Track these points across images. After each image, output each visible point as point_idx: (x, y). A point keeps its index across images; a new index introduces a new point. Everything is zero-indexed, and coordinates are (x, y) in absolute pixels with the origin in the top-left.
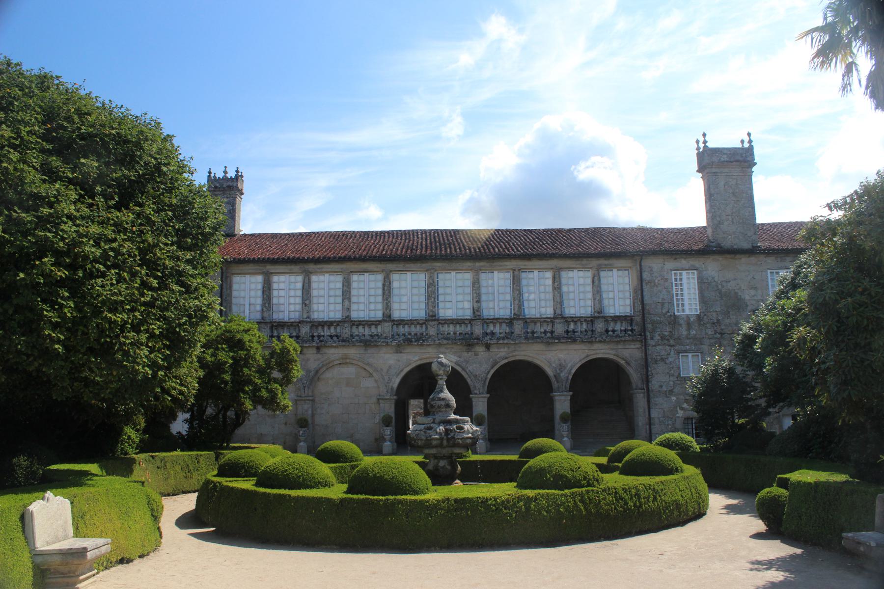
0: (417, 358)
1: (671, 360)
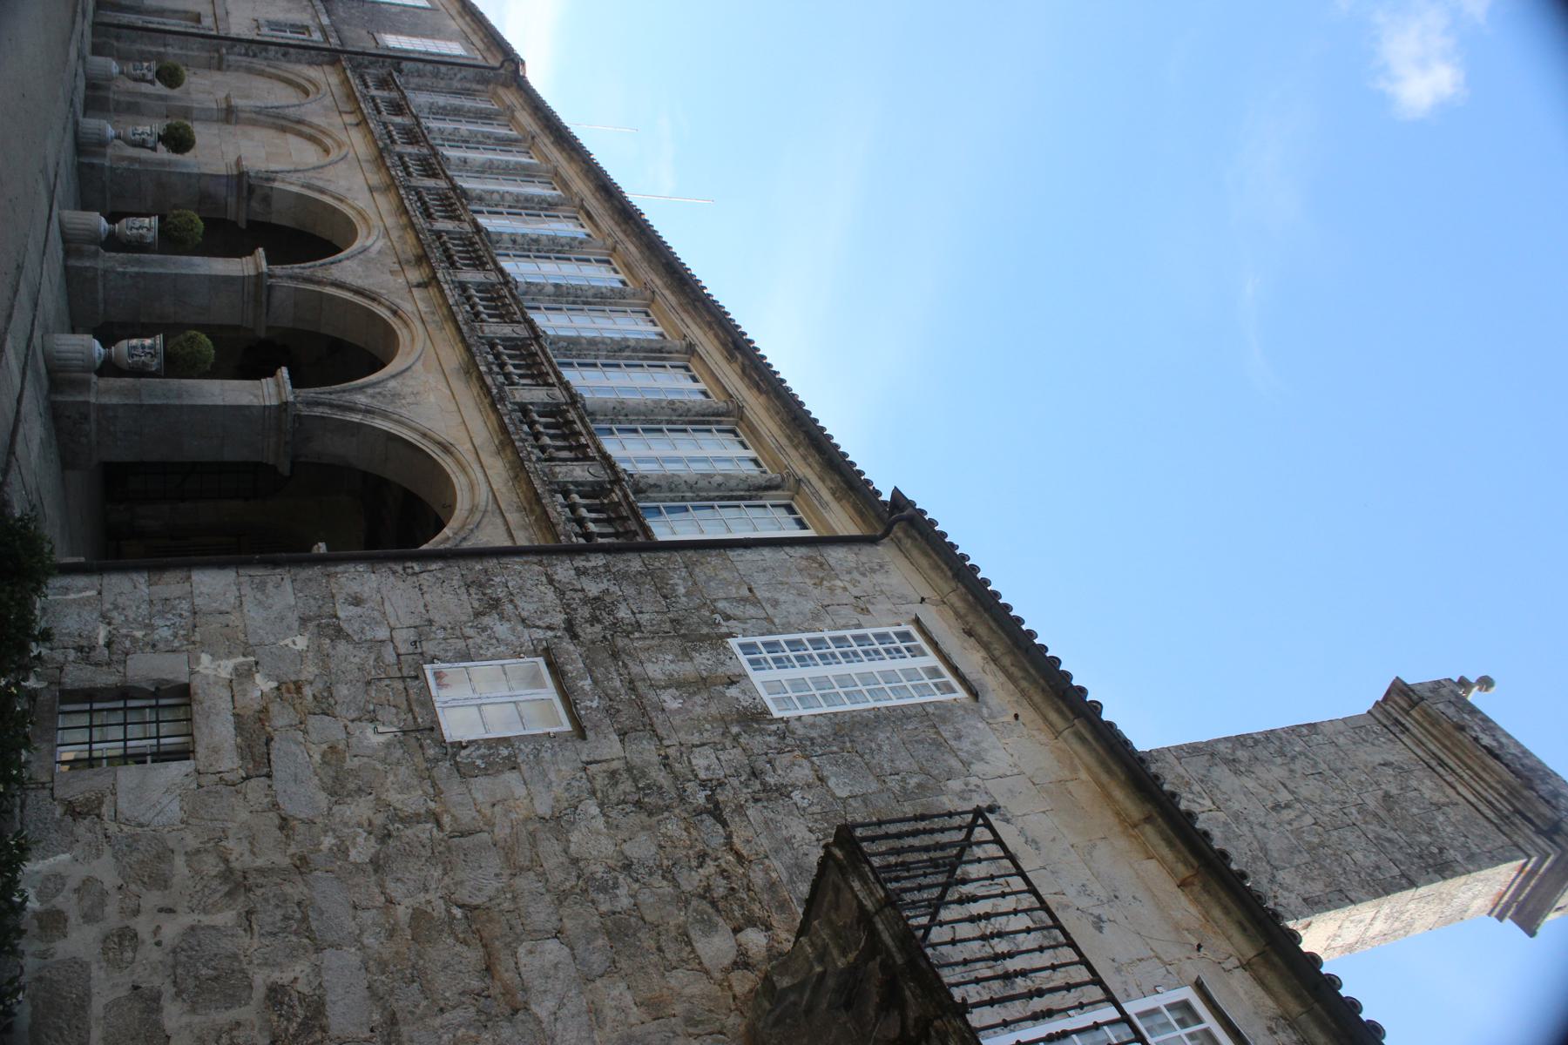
0: (360, 204)
1: (502, 629)
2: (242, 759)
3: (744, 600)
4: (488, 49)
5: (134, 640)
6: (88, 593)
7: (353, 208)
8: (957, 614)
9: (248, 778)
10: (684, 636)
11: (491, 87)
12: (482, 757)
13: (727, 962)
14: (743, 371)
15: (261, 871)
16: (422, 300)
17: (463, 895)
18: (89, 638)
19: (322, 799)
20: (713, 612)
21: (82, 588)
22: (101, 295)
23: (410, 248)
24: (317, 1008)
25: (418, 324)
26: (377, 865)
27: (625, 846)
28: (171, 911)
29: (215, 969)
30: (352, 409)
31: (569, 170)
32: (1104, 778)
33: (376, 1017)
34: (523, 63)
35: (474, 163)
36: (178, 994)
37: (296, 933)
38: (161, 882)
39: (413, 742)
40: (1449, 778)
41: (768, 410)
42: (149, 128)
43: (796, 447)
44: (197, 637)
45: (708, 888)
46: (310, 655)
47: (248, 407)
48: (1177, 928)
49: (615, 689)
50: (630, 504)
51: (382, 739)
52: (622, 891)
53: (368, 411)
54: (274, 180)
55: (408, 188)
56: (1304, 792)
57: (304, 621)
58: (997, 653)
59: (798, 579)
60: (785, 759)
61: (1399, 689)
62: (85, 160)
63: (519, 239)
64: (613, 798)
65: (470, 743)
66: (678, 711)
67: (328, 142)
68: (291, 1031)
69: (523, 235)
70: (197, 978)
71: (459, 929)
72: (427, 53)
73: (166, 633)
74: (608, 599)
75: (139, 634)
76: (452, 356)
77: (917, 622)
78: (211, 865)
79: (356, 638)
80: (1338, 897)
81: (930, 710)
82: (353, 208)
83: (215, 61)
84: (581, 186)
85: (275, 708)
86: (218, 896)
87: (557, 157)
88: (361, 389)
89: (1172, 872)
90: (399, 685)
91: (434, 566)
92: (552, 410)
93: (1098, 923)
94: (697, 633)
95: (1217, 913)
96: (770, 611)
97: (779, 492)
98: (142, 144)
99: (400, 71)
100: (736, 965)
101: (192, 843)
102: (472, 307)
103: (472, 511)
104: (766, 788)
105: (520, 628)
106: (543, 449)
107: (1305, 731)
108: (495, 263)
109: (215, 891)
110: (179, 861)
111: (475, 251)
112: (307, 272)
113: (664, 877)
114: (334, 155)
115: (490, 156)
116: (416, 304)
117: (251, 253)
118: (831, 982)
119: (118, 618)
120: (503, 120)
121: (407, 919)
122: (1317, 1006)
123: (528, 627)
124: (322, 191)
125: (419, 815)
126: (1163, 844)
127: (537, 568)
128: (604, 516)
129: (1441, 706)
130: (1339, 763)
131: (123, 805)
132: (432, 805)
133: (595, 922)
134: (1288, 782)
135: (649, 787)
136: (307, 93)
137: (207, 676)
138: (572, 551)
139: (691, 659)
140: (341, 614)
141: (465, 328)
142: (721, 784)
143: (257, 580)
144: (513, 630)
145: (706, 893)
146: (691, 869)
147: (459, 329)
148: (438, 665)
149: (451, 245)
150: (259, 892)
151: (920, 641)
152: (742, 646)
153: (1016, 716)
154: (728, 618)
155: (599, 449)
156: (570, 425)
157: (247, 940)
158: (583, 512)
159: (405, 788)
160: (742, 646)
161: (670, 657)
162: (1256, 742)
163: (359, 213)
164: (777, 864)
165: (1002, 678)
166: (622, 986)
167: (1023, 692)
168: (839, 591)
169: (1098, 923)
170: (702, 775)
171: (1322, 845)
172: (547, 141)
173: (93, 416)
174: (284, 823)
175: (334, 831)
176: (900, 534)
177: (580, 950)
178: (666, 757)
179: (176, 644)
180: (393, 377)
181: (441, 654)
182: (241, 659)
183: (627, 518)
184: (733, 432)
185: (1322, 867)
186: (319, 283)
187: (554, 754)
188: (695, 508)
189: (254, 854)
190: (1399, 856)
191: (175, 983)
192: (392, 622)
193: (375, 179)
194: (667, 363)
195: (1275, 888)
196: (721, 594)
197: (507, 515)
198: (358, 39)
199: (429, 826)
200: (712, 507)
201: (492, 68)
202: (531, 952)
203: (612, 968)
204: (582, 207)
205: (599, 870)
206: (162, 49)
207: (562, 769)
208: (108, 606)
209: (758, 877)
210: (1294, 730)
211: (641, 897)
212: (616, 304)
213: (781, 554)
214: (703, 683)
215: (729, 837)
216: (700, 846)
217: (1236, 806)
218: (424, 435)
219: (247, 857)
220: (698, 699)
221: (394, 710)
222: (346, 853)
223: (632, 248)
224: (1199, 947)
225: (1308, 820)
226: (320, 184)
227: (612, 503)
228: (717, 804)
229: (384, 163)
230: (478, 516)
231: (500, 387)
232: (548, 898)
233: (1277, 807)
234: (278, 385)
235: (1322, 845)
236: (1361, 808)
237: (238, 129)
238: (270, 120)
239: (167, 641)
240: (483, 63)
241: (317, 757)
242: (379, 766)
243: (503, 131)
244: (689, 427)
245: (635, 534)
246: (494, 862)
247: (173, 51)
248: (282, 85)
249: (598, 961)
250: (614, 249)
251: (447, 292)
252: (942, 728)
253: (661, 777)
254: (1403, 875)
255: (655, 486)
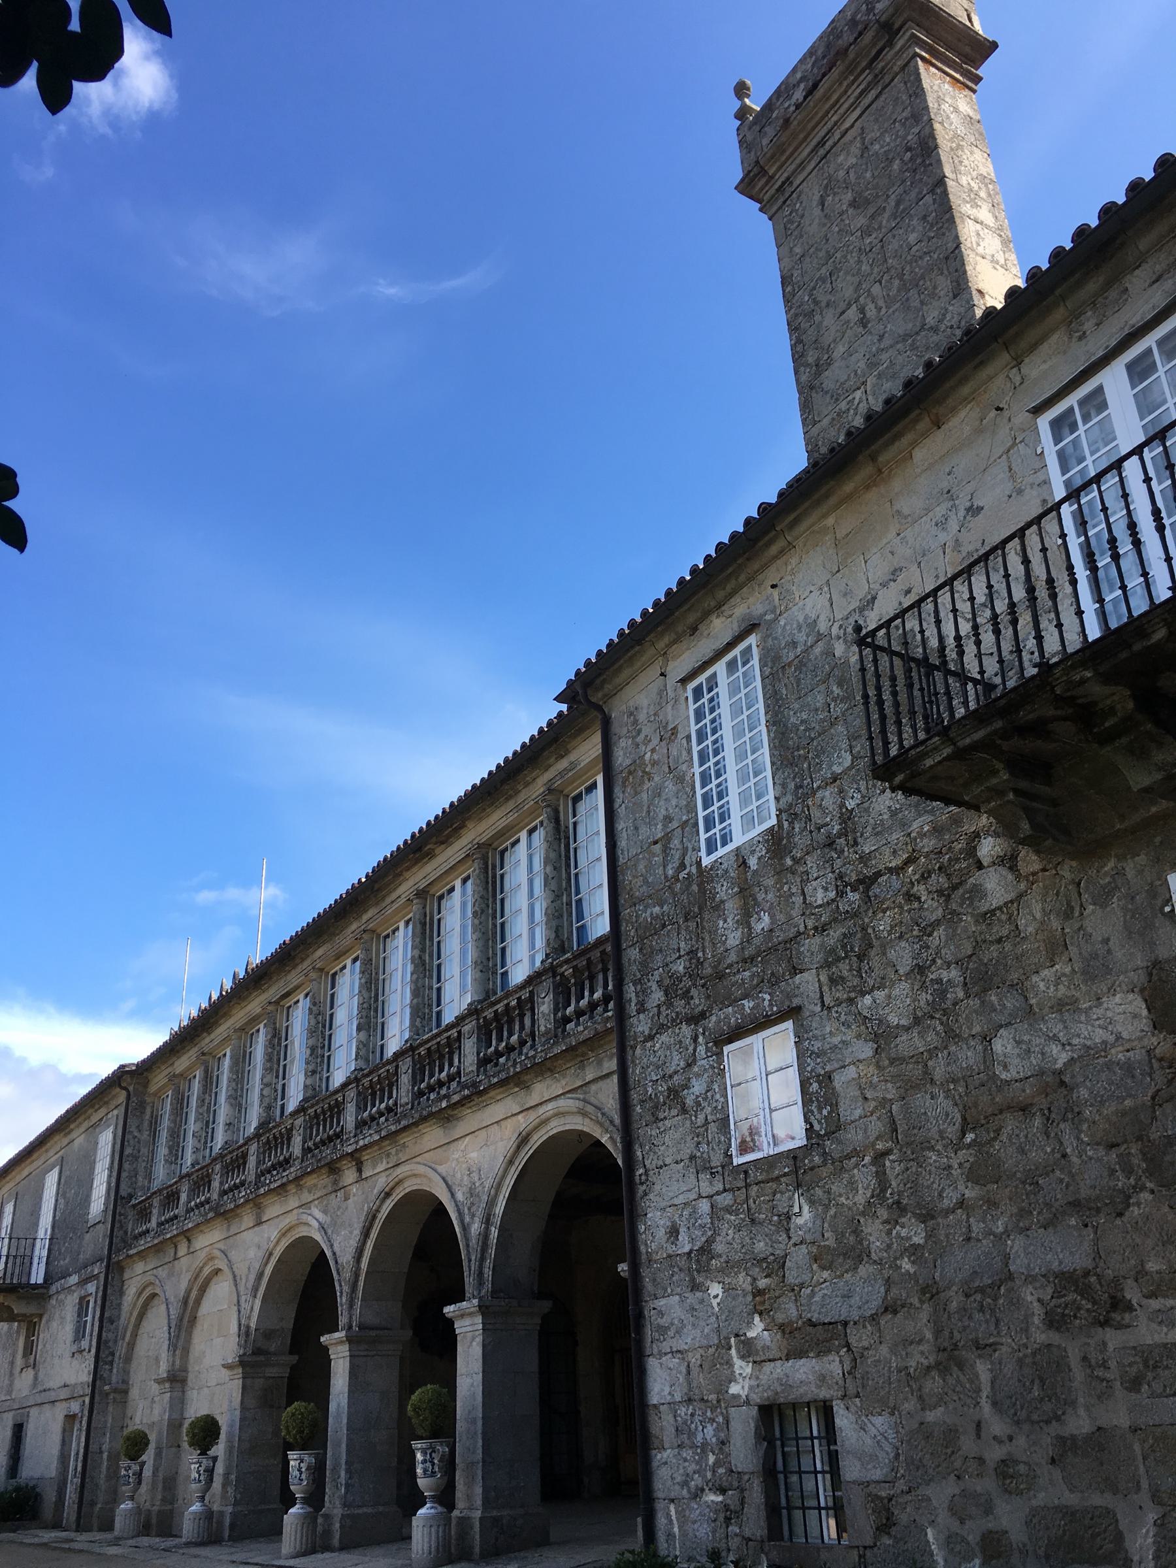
0: (274, 1235)
1: (698, 1087)
2: (829, 1351)
3: (666, 850)
4: (106, 1103)
5: (717, 1464)
6: (673, 1513)
7: (277, 1243)
8: (675, 642)
9: (848, 1345)
10: (700, 909)
11: (149, 1100)
12: (820, 1109)
13: (1010, 877)
14: (442, 843)
15: (937, 1333)
16: (374, 1167)
17: (952, 1131)
18: (716, 1512)
19: (864, 1270)
20: (678, 880)
21: (668, 1518)
22: (369, 1510)
23: (321, 1181)
24: (1067, 1280)
25: (399, 1170)
26: (927, 1216)
27: (901, 972)
28: (979, 1425)
29: (1033, 1382)
30: (485, 1235)
31: (238, 1017)
32: (833, 500)
33: (1073, 1222)
34: (122, 1067)
35: (231, 1116)
36: (1058, 1418)
37: (995, 1299)
38: (951, 1435)
39: (807, 1178)
40: (837, 136)
41: (480, 820)
42: (191, 1464)
43: (518, 792)
44: (713, 1397)
45: (940, 892)
46: (727, 1280)
47: (484, 1346)
48: (979, 431)
49: (752, 977)
50: (575, 957)
51: (806, 1208)
52: (945, 975)
53: (487, 1221)
54: (248, 1327)
55: (258, 1184)
56: (849, 293)
57: (695, 1287)
58: (713, 604)
59: (644, 796)
60: (816, 813)
61: (746, 187)
62: (226, 1534)
63: (311, 1068)
64: (856, 981)
65: (807, 1120)
66: (772, 916)
67: (207, 1271)
68: (1090, 1306)
69: (307, 1063)
70: (1042, 1399)
71: (985, 1137)
72: (111, 1169)
73: (710, 1430)
74: (667, 982)
75: (712, 1459)
76: (432, 1135)
77: (684, 681)
78: (933, 1384)
79: (710, 1233)
80: (952, 262)
81: (767, 671)
82: (277, 1243)
83: (118, 1397)
84: (255, 1004)
85: (780, 1317)
86: (962, 1377)
87: (223, 1030)
88: (465, 1228)
89: (925, 435)
90: (754, 1190)
91: (639, 1153)
92: (485, 1034)
93: (974, 511)
94: (696, 895)
95: (966, 390)
96: (675, 824)
97: (561, 808)
98: (210, 1472)
99: (131, 1196)
100: (1013, 868)
101: (910, 1405)
102: (381, 1114)
103: (583, 1114)
104: (843, 833)
105: (696, 1069)
106: (522, 1043)
107: (789, 289)
108: (337, 1091)
109: (958, 1381)
110: (931, 1416)
111: (324, 1112)
112: (346, 1288)
113: (930, 935)
114: (221, 1264)
115: (222, 1098)
116: (379, 1174)
117: (326, 1349)
118: (1023, 784)
119: (697, 1481)
120: (183, 1085)
121: (977, 1188)
122: (1058, 292)
123: (695, 1061)
124: (260, 1275)
125: (877, 1172)
126: (897, 444)
127: (638, 1051)
128: (587, 984)
129: (765, 142)
130: (822, 254)
131: (877, 1474)
132: (867, 1159)
133: (974, 1003)
134: (839, 310)
135: (844, 947)
136: (154, 1295)
137: (751, 1388)
138: (621, 1016)
139: (723, 902)
140: (687, 1249)
141: (404, 1123)
142: (841, 877)
143: (656, 1335)
144: (698, 1075)
145: (944, 895)
146: (921, 908)
147: (405, 1128)
148: (734, 1150)
149: (320, 1137)
150: (957, 1336)
151: (702, 679)
152: (709, 853)
153: (773, 586)
154: (682, 866)
155: (522, 987)
156: (499, 1014)
157: (1004, 1349)
158: (583, 1003)
159: (852, 1186)
160: (709, 853)
161: (721, 923)
162: (799, 341)
163: (284, 1235)
164: (915, 825)
165: (736, 600)
166: (1035, 978)
167: (751, 579)
168: (656, 757)
169: (974, 511)
170: (832, 895)
171: (901, 276)
172: (207, 1040)
173: (495, 1513)
174: (890, 1308)
175: (896, 1259)
176: (600, 695)
177: (1003, 1019)
178: (816, 928)
179: (720, 1419)
180: (453, 1195)
181: (723, 1147)
182: (733, 1352)
183: (589, 960)
184: (503, 853)
185: (923, 277)
186: (357, 1276)
187: (816, 1037)
188: (578, 892)
189: (921, 1341)
190: (913, 195)
191: (1048, 1422)
192: (693, 1196)
193: (248, 1219)
194: (436, 918)
195: (943, 327)
196: (660, 871)
197: (589, 1077)
198: (95, 1242)
199: (888, 1163)
200: (577, 875)
201: (128, 1098)
202: (1005, 1067)
203: (1020, 988)
204: (277, 1002)
205: (925, 997)
206: (105, 1455)
207: (830, 1031)
208: (685, 1492)
209: (928, 844)
210: (787, 299)
211: (949, 958)
212: (377, 968)
213: (621, 811)
214: (746, 892)
215: (890, 870)
216: (900, 899)
217: (862, 364)
218: (511, 1162)
219: (924, 1347)
220: (760, 896)
221: (778, 1196)
222: (916, 1247)
223: (319, 952)
224: (998, 409)
225: (876, 289)
226: (252, 1277)
227: (574, 975)
228: (860, 881)
229: (232, 1210)
230: (589, 1109)
231: (464, 1086)
232: (953, 1048)
233: (863, 322)
234: (462, 1316)
235: (901, 276)
236: (866, 232)
237: (193, 1368)
238: (183, 1334)
239: (717, 1430)
240: (123, 1109)
241: (826, 1274)
242: (832, 1212)
243: (196, 1085)
244: (499, 897)
245: (603, 952)
246: (921, 1101)
247: (106, 1443)
248: (144, 1323)
249: (1011, 1002)
250: (321, 970)
251: (366, 1141)
252: (785, 660)
253: (835, 934)
254: (932, 191)
255: (556, 932)
